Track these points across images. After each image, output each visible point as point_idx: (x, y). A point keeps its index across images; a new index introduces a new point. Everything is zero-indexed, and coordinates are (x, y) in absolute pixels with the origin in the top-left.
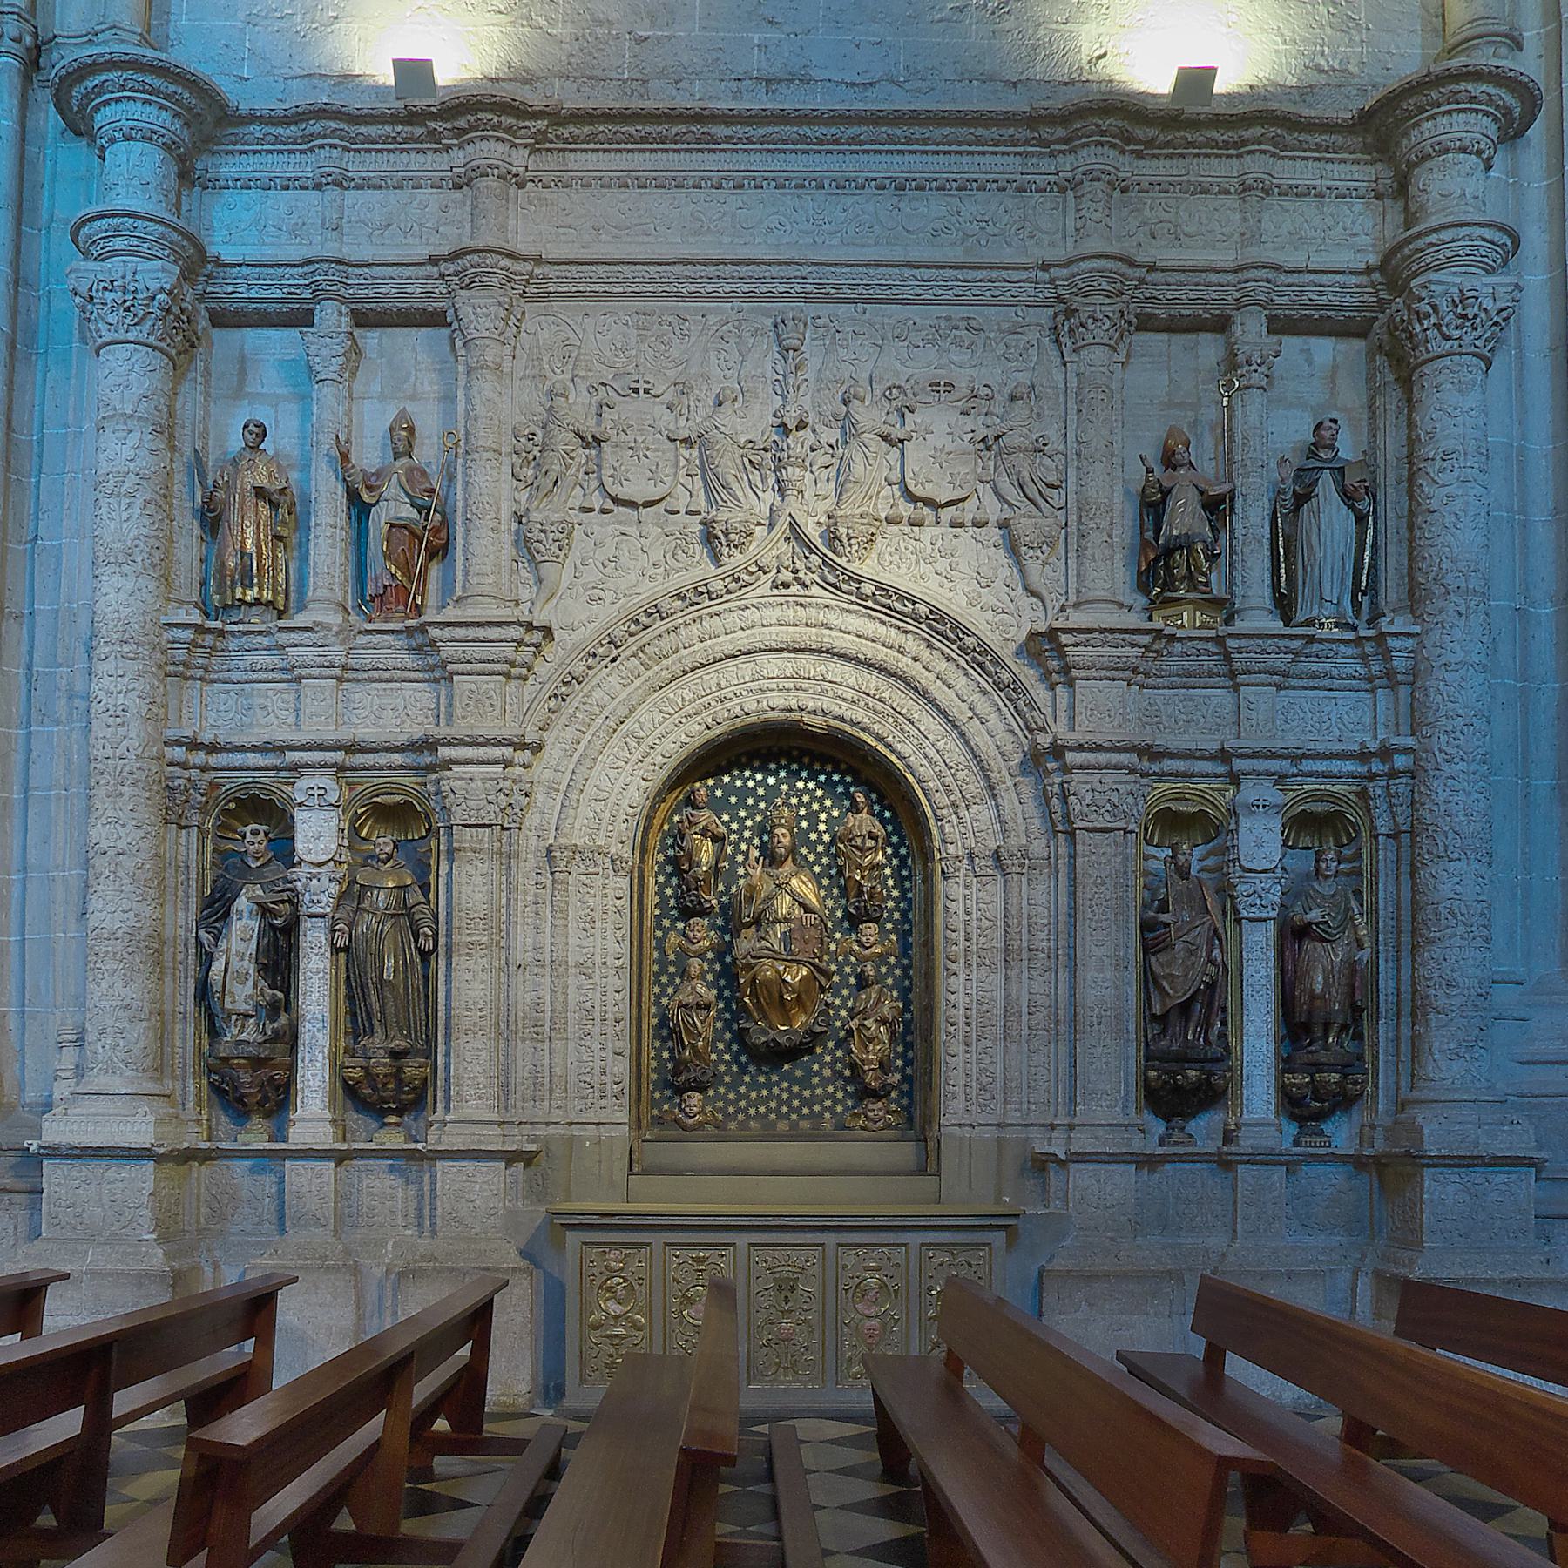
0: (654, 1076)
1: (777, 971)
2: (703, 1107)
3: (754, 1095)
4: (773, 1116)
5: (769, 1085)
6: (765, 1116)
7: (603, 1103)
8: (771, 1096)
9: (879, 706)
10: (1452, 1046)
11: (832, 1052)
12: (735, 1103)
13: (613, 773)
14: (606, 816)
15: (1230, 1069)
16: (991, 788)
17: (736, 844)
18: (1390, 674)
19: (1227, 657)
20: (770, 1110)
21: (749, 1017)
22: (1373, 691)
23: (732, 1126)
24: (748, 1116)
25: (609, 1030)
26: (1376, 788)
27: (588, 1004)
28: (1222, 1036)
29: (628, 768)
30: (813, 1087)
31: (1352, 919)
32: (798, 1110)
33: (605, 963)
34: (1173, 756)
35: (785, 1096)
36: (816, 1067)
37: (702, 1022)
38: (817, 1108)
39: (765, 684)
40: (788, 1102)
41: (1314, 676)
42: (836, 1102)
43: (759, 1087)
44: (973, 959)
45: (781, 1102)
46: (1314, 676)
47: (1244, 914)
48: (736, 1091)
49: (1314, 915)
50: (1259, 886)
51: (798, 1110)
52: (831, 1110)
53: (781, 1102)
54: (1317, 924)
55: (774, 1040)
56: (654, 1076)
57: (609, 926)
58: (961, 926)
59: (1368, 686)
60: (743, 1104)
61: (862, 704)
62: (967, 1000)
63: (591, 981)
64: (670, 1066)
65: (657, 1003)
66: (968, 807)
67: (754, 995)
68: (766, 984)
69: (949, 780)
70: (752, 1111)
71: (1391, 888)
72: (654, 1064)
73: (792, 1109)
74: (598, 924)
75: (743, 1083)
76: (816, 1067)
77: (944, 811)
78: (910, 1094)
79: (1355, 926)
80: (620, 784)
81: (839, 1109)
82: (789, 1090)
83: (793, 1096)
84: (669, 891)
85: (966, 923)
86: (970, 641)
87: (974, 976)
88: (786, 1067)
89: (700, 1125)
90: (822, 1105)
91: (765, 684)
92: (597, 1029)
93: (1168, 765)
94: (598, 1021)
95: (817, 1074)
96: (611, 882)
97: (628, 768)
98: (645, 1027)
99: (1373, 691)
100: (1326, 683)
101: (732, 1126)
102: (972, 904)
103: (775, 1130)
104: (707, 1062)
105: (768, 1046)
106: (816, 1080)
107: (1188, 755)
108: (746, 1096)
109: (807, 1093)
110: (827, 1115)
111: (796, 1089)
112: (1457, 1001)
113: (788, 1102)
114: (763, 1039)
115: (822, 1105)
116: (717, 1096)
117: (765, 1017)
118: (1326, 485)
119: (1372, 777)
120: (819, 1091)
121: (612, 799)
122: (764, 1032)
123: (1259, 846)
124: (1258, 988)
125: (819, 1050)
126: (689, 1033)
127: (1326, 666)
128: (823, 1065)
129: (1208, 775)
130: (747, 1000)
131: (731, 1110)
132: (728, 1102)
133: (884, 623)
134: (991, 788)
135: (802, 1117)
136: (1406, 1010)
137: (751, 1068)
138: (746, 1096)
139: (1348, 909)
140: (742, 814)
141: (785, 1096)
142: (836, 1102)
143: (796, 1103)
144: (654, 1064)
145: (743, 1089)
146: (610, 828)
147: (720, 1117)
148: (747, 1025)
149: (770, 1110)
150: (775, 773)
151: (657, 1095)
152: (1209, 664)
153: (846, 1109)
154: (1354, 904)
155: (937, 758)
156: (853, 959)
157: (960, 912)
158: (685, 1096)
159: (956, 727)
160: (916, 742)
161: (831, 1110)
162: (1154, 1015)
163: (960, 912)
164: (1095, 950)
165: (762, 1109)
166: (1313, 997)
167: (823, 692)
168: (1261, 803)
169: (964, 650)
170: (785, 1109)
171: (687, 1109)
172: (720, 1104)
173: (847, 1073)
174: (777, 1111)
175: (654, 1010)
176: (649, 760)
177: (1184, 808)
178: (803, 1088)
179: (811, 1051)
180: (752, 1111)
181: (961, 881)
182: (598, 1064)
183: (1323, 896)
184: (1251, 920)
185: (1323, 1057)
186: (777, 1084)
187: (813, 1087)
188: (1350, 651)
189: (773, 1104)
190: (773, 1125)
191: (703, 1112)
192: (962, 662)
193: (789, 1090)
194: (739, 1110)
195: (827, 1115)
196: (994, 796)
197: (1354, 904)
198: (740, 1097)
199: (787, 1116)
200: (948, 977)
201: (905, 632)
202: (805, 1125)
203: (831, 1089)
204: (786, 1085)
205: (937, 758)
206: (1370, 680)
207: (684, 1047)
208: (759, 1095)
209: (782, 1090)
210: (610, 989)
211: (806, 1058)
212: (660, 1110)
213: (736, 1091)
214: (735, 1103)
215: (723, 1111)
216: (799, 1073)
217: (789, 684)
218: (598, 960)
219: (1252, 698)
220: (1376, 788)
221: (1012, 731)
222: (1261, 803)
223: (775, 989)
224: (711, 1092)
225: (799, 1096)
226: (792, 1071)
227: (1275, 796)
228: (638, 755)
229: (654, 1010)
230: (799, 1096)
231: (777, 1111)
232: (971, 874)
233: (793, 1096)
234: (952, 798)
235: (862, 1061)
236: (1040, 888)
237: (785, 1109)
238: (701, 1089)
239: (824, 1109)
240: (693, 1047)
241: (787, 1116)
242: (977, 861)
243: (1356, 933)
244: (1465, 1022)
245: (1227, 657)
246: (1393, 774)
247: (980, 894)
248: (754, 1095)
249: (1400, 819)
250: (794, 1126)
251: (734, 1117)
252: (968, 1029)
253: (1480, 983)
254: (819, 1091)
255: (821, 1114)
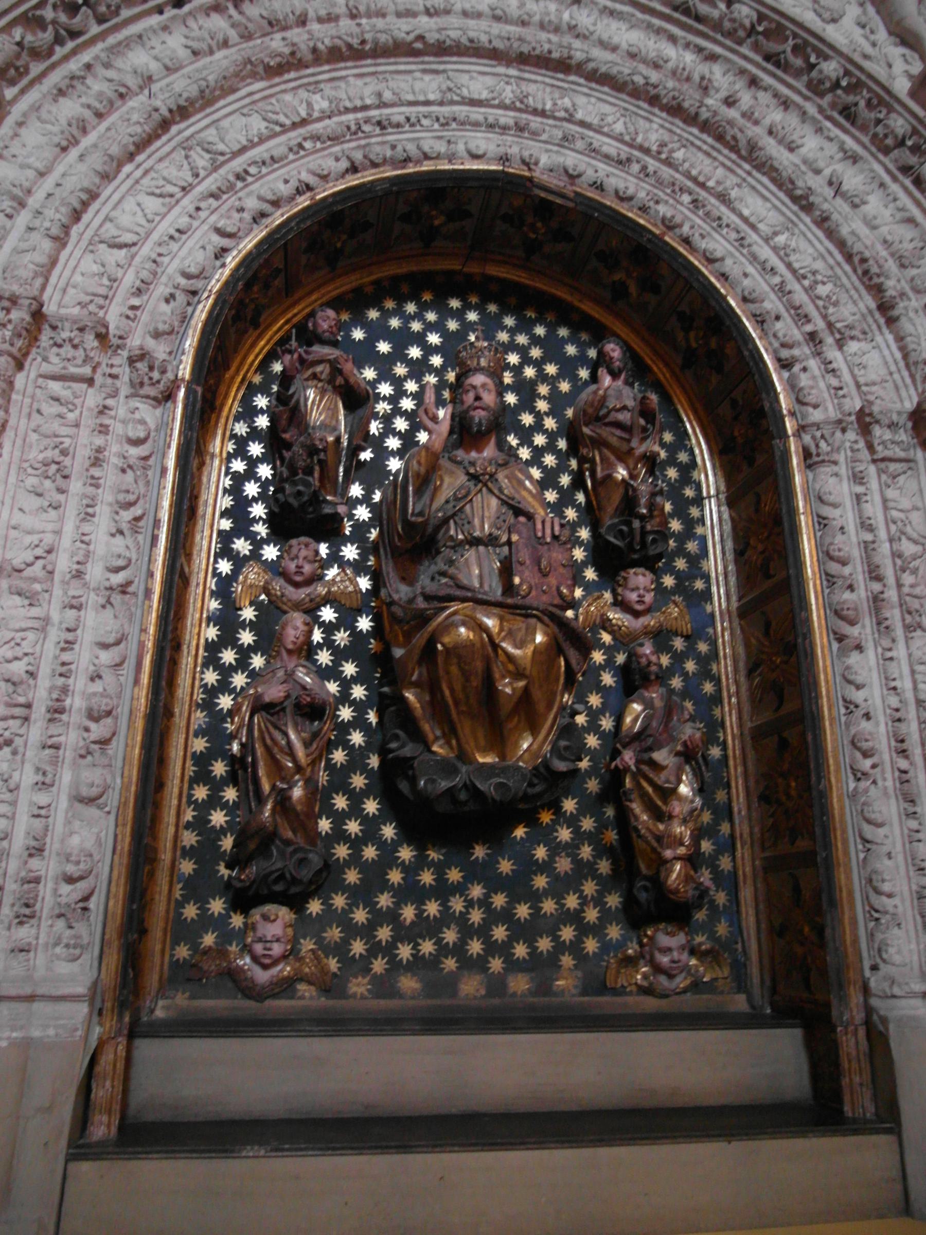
0: (187, 867)
1: (483, 628)
2: (295, 941)
3: (408, 913)
4: (450, 964)
5: (442, 891)
6: (434, 962)
7: (24, 933)
8: (446, 917)
9: (666, 172)
11: (572, 822)
12: (367, 931)
13: (153, 204)
14: (129, 279)
16: (885, 308)
17: (387, 419)
20: (443, 950)
21: (417, 735)
23: (359, 986)
24: (395, 965)
25: (71, 739)
27: (19, 668)
29: (188, 203)
30: (535, 898)
32: (504, 949)
33: (79, 575)
35: (476, 916)
36: (541, 853)
37: (307, 744)
38: (544, 944)
39: (461, 111)
40: (483, 932)
42: (584, 930)
43: (418, 895)
44: (894, 616)
45: (467, 931)
48: (370, 905)
51: (504, 949)
52: (575, 948)
53: (467, 931)
55: (470, 787)
56: (187, 867)
57: (106, 496)
58: (856, 553)
60: (384, 934)
61: (636, 168)
62: (894, 701)
63: (35, 612)
64: (227, 843)
65: (209, 705)
66: (840, 344)
67: (431, 687)
68: (457, 652)
69: (800, 297)
70: (405, 952)
72: (189, 838)
73: (492, 948)
74: (76, 486)
75: (385, 886)
76: (541, 853)
77: (796, 352)
78: (734, 910)
80: (165, 227)
81: (591, 945)
82: (484, 903)
83: (493, 917)
84: (251, 489)
85: (868, 548)
86: (831, 68)
87: (900, 651)
88: (480, 852)
89: (285, 987)
90: (556, 938)
91: (461, 111)
92: (36, 732)
94: (39, 712)
95: (546, 867)
96: (121, 405)
97: (188, 203)
98: (176, 753)
101: (359, 986)
102: (873, 509)
103: (454, 993)
104: (313, 836)
105: (455, 801)
106: (541, 882)
108: (392, 917)
109: (523, 911)
110: (567, 961)
111: (499, 900)
113: (483, 932)
114: (444, 784)
115: (556, 938)
116: (329, 916)
117: (450, 732)
120: (549, 906)
121: (146, 250)
122: (447, 768)
125: (546, 818)
126: (276, 767)
128: (556, 849)
130: (409, 695)
131: (358, 947)
132: (351, 930)
133: (673, 39)
134: (885, 308)
135: (513, 965)
137: (406, 854)
138: (392, 917)
140: (400, 370)
141: (476, 916)
142: (584, 930)
143: (500, 933)
144: (189, 838)
145: (384, 901)
146: (136, 302)
147: (333, 964)
148: (408, 751)
149: (443, 950)
150: (459, 315)
151: (191, 911)
153: (606, 947)
155: (775, 261)
156: (606, 638)
157: (851, 527)
158: (256, 915)
159: (808, 208)
160: (734, 235)
161: (575, 948)
163: (851, 527)
165: (427, 947)
167: (566, 140)
169: (816, 88)
170: (475, 947)
171: (259, 948)
172: (334, 933)
173: (604, 867)
174: (459, 950)
175: (200, 717)
176: (233, 201)
178: (514, 899)
179: (531, 821)
180: (405, 952)
181: (843, 470)
182: (23, 825)
186: (460, 889)
187: (535, 898)
189: (450, 936)
190: (451, 983)
191: (292, 953)
192: (811, 109)
193: (484, 903)
194: (375, 949)
195: (567, 961)
196: (891, 321)
198: (378, 917)
199: (480, 964)
200: (844, 652)
201: (712, 58)
202: (520, 984)
203: (572, 902)
204: (477, 891)
205: (775, 261)
207: (261, 800)
208: (419, 914)
209: (470, 904)
210: (86, 637)
211: (520, 832)
212: (195, 947)
213: (370, 905)
214: (367, 931)
215: (341, 950)
216: (505, 866)
217: (507, 118)
218: (63, 563)
221: (911, 221)
223: (479, 665)
224: (315, 907)
225: (506, 916)
226: (491, 863)
228: (210, 183)
229: (200, 717)
230: (506, 916)
231: (459, 950)
232: (865, 455)
233: (493, 917)
234: (809, 328)
235: (659, 838)
237: (475, 947)
238: (297, 903)
239: (560, 947)
240: (283, 802)
241: (480, 964)
242: (877, 431)
247: (891, 493)
248: (408, 913)
250: (497, 986)
251: (363, 965)
252: (903, 764)
254: (549, 906)
255: (552, 961)
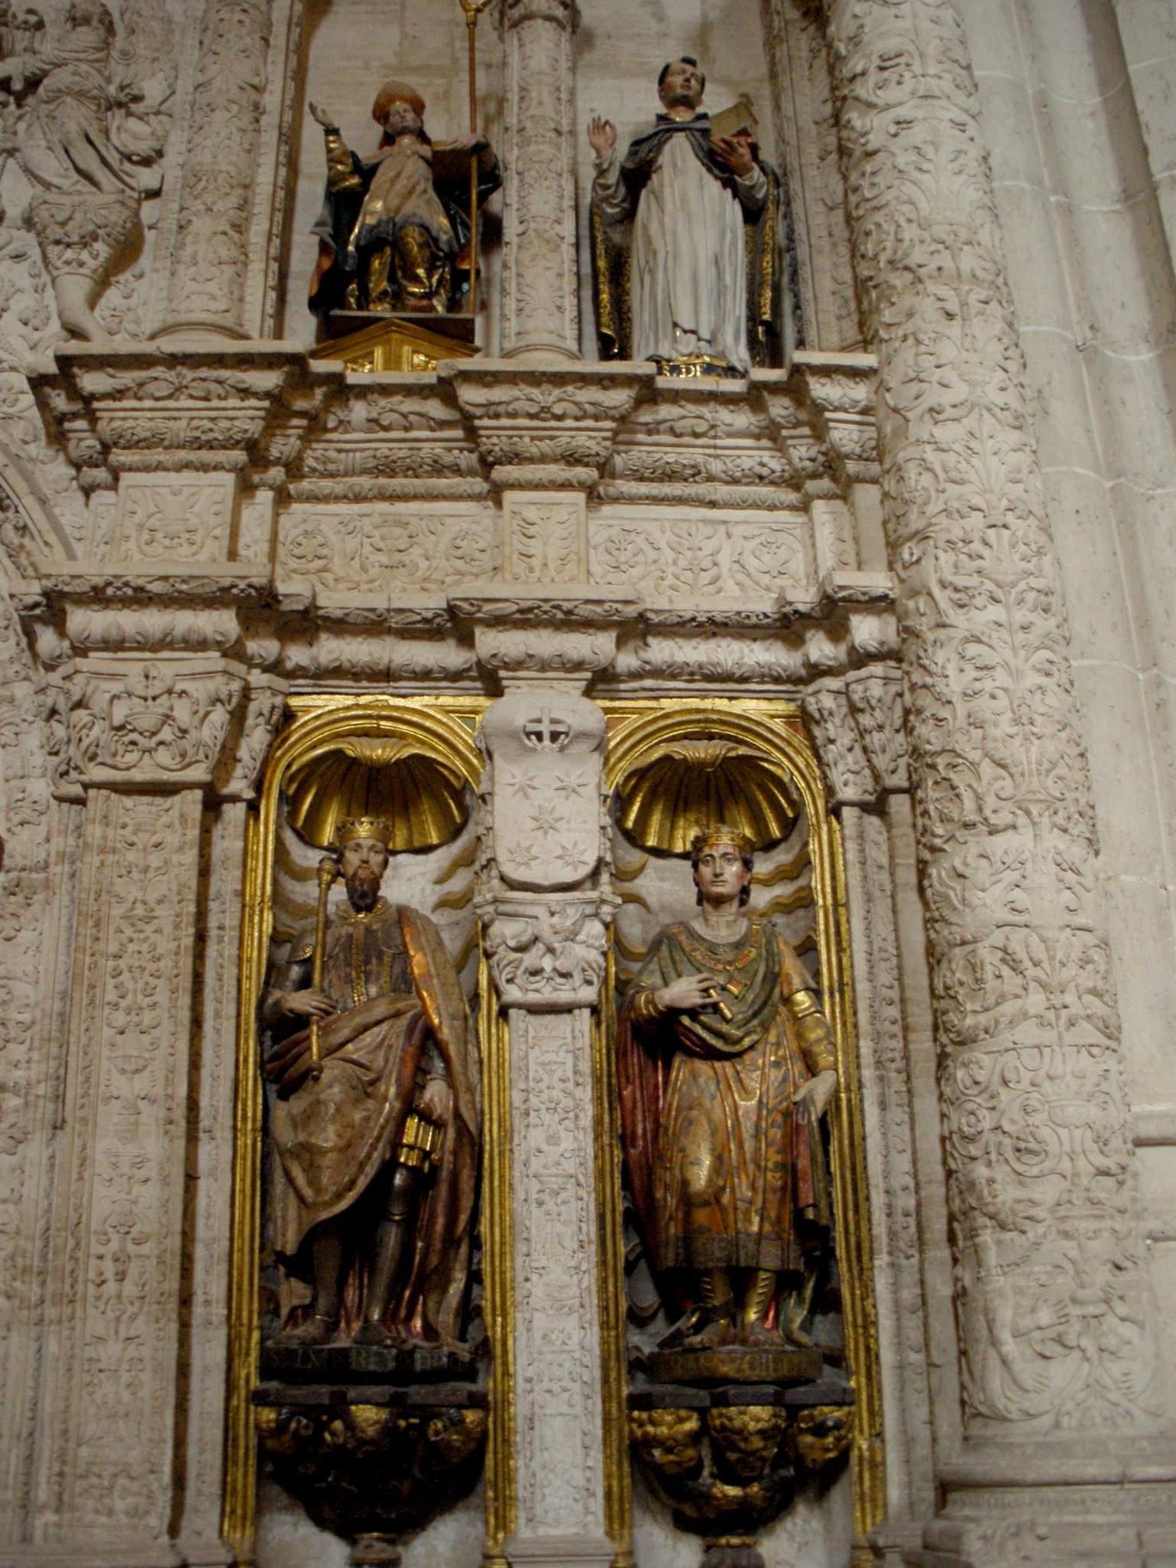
10: (1045, 1316)
15: (478, 1401)
18: (831, 465)
19: (467, 423)
22: (804, 507)
26: (824, 697)
28: (469, 1312)
31: (788, 1001)
34: (341, 626)
41: (670, 475)
46: (670, 475)
47: (512, 994)
49: (683, 991)
50: (545, 925)
54: (693, 1013)
59: (791, 497)
71: (883, 928)
79: (797, 1020)
93: (330, 649)
99: (804, 507)
100: (702, 489)
107: (375, 625)
112: (1047, 1192)
118: (679, 158)
119: (815, 672)
123: (544, 825)
124: (554, 1183)
127: (691, 455)
129: (426, 675)
136: (938, 1227)
139: (773, 977)
152: (433, 446)
154: (792, 968)
162: (281, 1257)
164: (120, 1085)
166: (688, 1201)
168: (545, 728)
177: (378, 752)
183: (712, 948)
184: (536, 1010)
185: (727, 1362)
188: (743, 419)
197: (792, 968)
206: (794, 481)
219: (531, 514)
220: (824, 697)
222: (545, 728)
227: (586, 714)
236: (26, 937)
243: (799, 1036)
244: (1070, 1247)
245: (467, 423)
246: (860, 659)
249: (881, 762)
253: (1101, 1142)
